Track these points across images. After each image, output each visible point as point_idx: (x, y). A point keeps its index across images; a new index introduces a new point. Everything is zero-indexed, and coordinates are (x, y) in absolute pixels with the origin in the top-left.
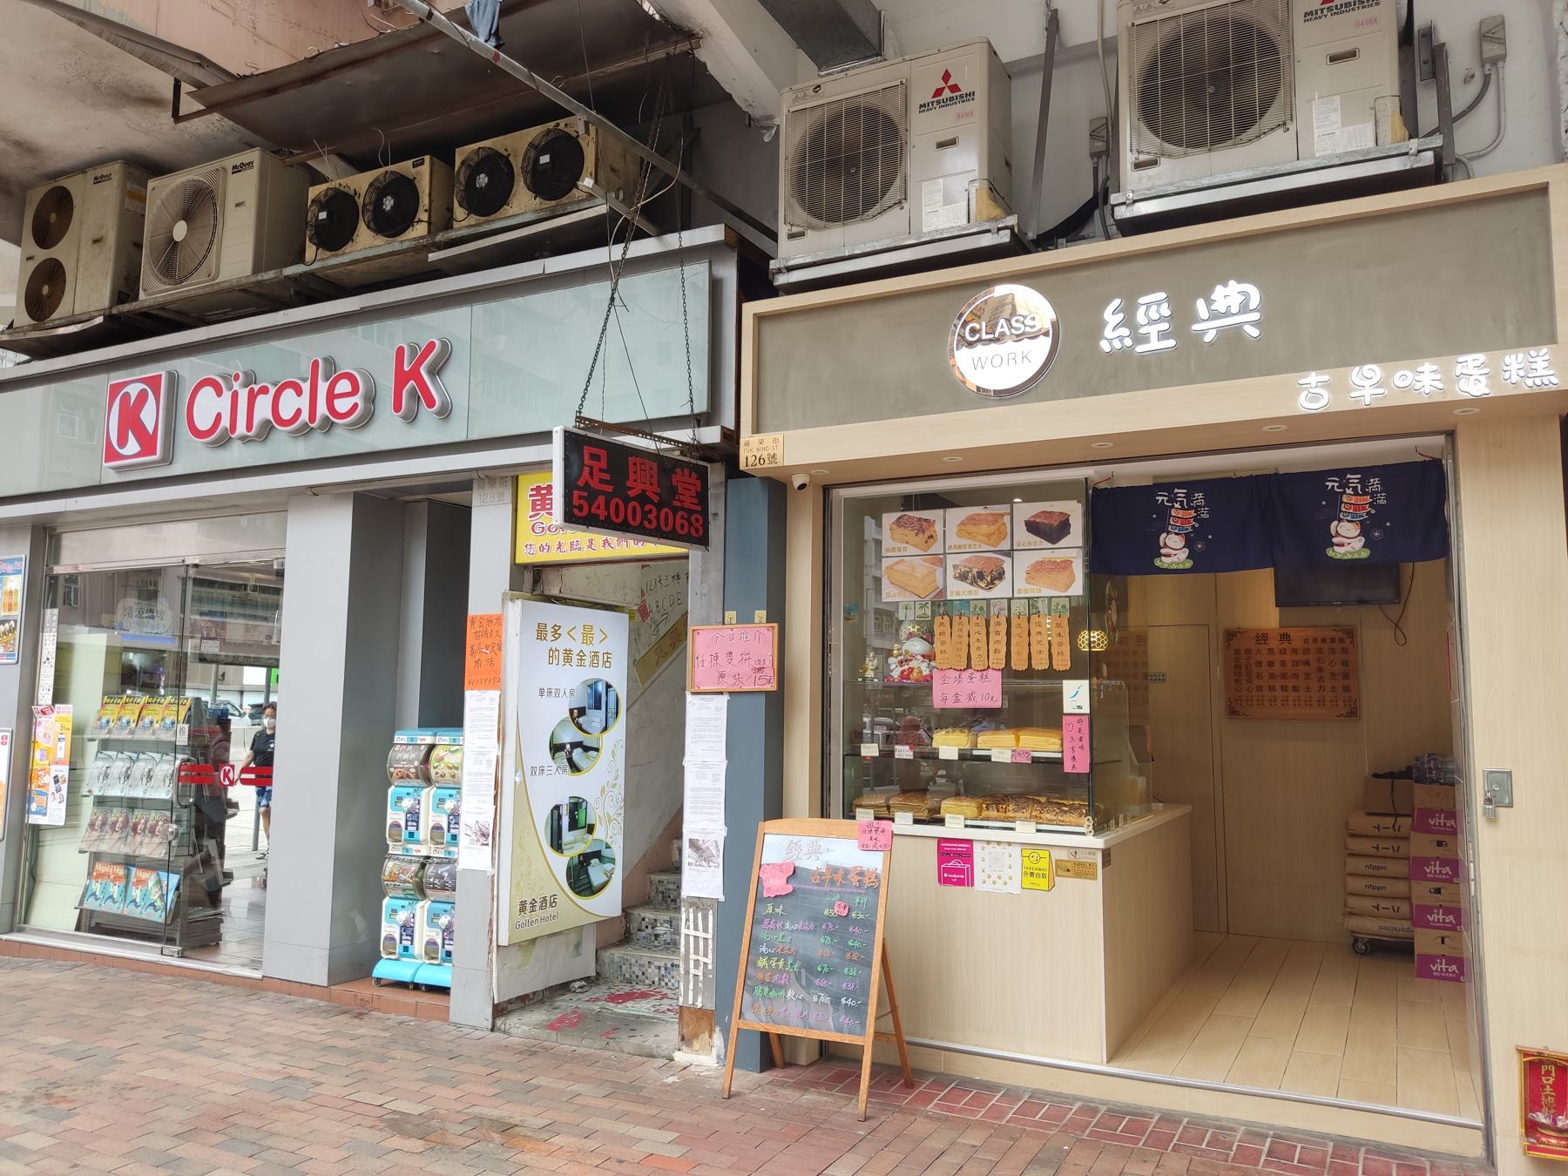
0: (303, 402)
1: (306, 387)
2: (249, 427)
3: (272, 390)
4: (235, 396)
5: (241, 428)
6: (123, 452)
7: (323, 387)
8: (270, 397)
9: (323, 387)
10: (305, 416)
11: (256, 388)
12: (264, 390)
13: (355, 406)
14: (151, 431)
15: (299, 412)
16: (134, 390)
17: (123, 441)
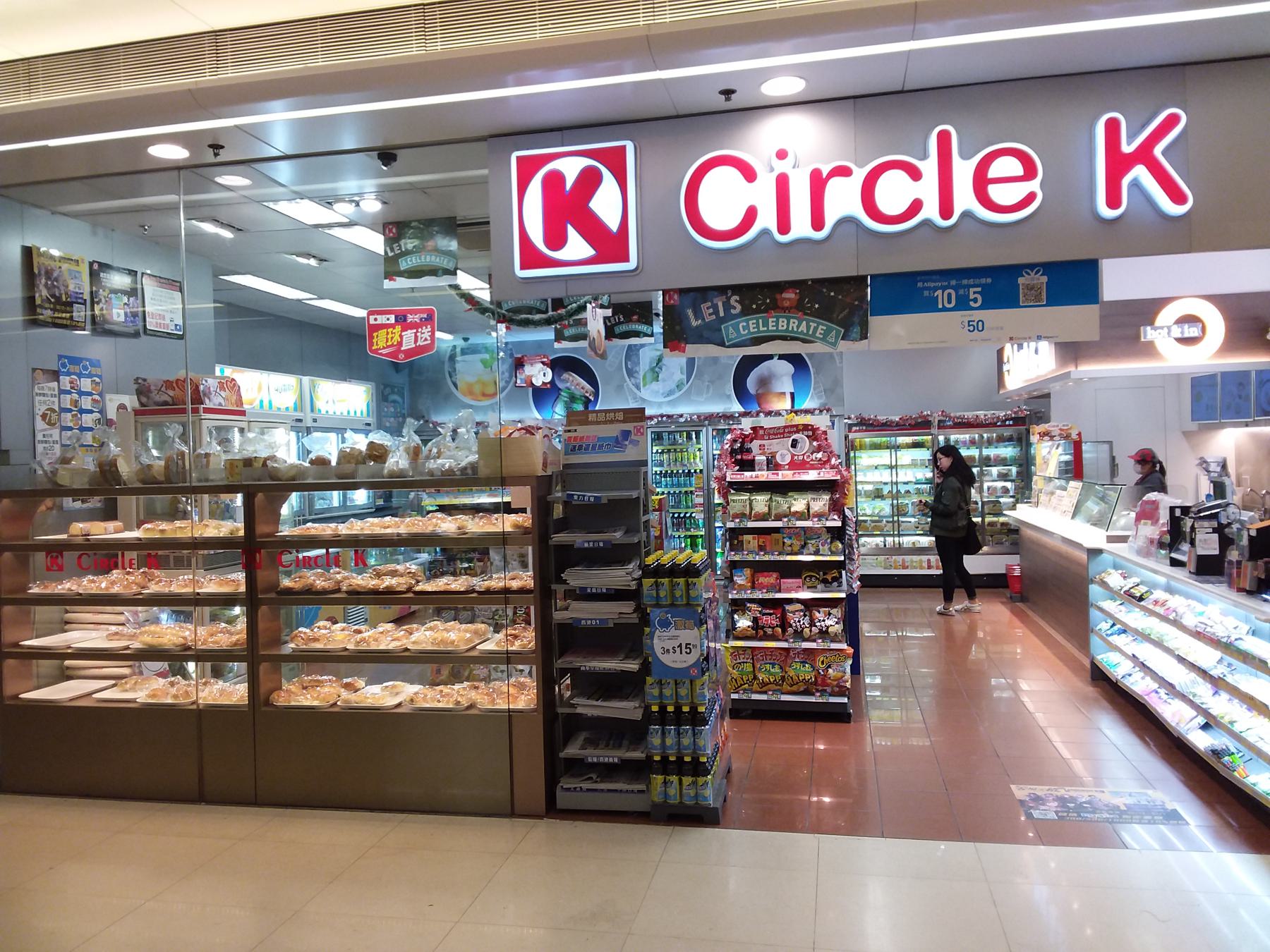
0: (928, 190)
1: (930, 167)
2: (818, 223)
3: (860, 174)
5: (801, 226)
7: (963, 171)
9: (963, 171)
10: (930, 210)
12: (844, 172)
13: (1031, 197)
14: (613, 225)
15: (916, 206)
16: (571, 168)
17: (556, 239)
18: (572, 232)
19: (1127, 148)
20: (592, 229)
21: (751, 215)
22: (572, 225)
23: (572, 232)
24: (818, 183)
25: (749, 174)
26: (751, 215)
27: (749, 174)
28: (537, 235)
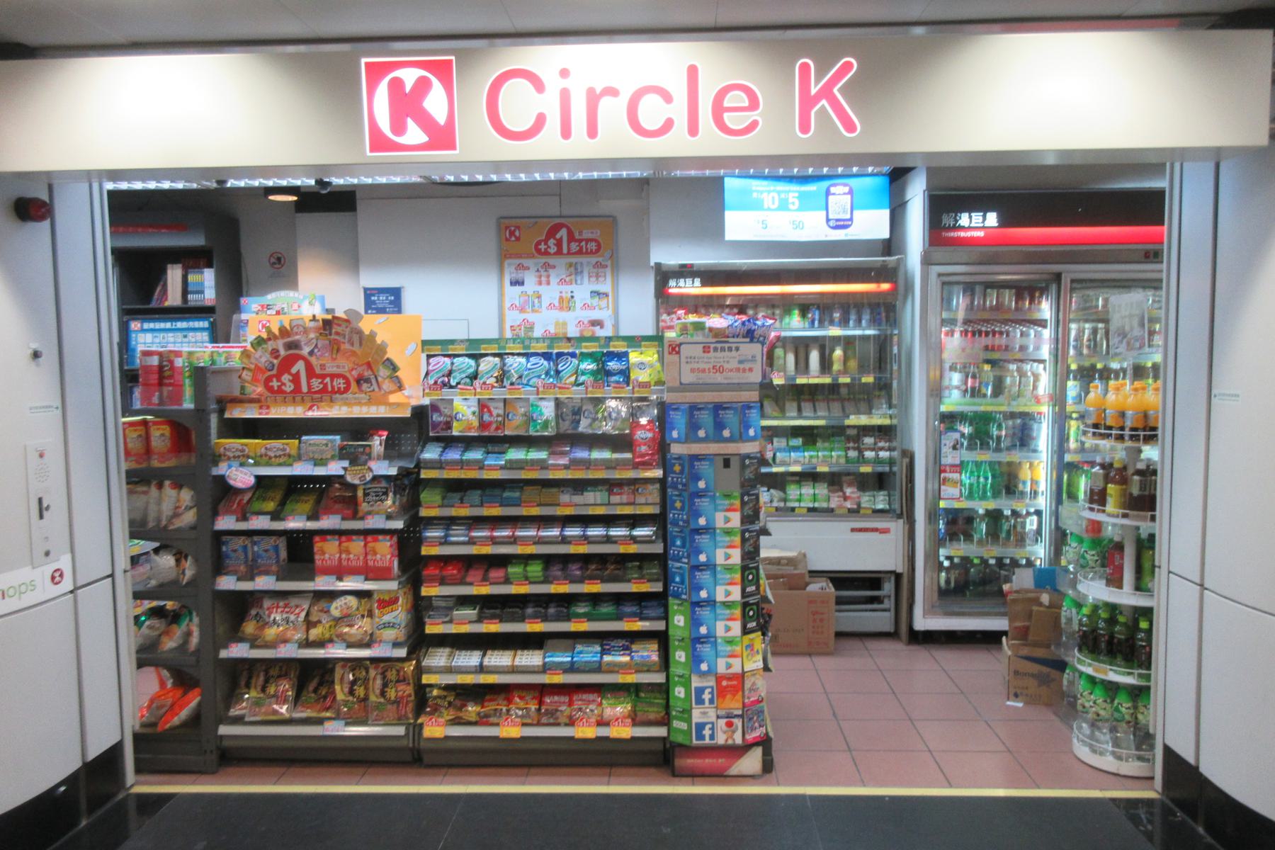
4: (565, 96)
6: (401, 140)
8: (622, 102)
11: (598, 91)
12: (612, 92)
14: (441, 118)
17: (399, 128)
18: (410, 123)
19: (814, 91)
20: (426, 121)
21: (540, 121)
22: (412, 118)
23: (410, 122)
24: (593, 99)
25: (539, 85)
26: (540, 121)
27: (539, 85)
28: (384, 124)
